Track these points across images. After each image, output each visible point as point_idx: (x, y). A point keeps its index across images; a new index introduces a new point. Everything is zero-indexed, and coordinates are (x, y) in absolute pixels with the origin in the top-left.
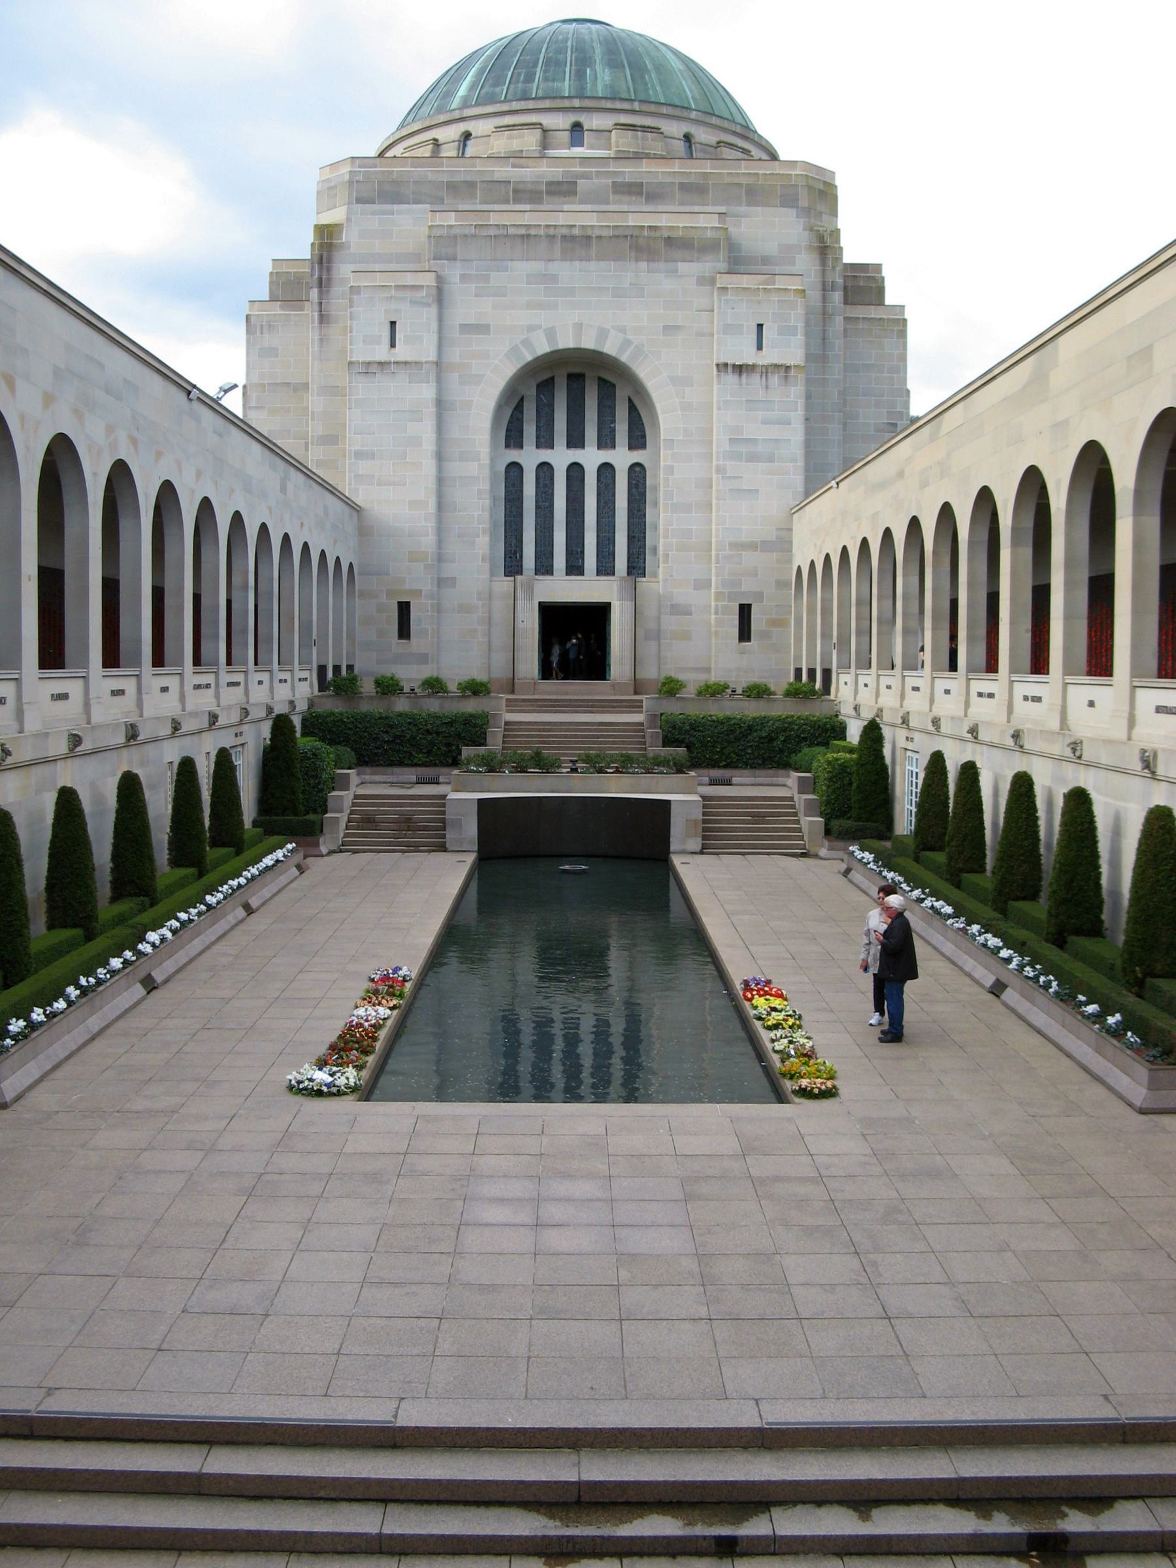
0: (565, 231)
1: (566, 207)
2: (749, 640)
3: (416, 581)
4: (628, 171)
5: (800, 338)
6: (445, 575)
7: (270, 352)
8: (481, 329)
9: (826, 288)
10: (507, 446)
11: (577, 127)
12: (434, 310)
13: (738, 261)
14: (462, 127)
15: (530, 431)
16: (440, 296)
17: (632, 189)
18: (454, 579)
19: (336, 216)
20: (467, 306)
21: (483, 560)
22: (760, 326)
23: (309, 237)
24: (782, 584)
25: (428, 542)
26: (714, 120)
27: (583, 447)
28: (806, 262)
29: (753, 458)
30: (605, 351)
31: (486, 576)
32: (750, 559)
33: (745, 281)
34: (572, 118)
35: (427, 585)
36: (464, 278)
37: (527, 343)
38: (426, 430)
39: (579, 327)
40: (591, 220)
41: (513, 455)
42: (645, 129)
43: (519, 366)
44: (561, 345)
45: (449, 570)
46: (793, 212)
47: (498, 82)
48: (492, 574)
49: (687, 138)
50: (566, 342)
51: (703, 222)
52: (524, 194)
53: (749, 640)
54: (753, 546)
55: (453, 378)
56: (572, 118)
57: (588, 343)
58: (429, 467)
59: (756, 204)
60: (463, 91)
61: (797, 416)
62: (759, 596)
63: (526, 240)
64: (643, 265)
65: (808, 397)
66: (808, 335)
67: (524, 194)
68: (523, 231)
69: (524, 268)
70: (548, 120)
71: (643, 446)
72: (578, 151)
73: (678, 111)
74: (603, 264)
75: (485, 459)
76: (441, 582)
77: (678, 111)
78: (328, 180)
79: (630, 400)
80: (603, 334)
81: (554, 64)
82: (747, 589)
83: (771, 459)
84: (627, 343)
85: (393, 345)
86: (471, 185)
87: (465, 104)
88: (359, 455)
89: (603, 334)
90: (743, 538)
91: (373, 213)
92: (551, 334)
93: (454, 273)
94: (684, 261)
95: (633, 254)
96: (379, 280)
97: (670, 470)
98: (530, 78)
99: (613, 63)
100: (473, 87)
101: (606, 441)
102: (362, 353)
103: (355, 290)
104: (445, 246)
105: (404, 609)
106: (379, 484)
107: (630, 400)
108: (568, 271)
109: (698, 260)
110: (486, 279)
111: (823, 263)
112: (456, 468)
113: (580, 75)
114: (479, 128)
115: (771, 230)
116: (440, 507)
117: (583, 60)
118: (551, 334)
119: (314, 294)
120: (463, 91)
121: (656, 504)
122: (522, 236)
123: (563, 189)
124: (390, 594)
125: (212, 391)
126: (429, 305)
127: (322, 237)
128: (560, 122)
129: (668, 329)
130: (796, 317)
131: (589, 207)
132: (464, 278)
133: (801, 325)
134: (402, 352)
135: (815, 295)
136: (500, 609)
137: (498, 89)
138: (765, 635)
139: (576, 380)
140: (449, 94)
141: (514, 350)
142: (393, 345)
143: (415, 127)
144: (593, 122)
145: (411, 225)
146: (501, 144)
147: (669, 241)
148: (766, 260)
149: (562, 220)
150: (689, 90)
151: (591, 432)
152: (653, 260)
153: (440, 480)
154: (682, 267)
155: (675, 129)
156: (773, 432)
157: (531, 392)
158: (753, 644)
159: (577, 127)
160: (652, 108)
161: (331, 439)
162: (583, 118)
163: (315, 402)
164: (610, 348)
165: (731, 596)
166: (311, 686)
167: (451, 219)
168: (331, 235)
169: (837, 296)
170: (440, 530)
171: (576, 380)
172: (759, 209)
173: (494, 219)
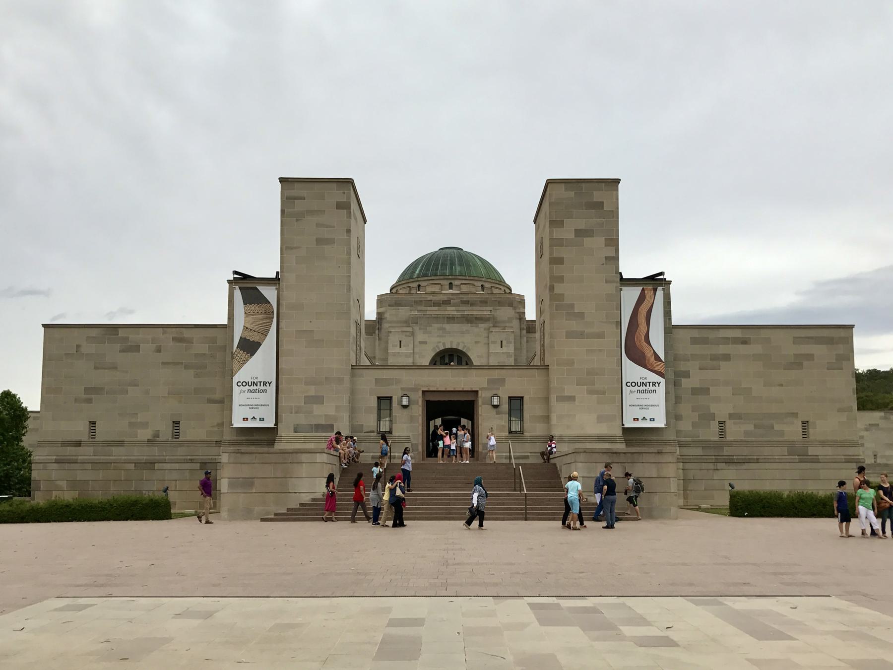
1: (448, 308)
4: (465, 298)
8: (425, 343)
9: (521, 329)
11: (451, 284)
13: (495, 322)
16: (413, 334)
20: (420, 337)
28: (516, 323)
33: (497, 329)
36: (420, 329)
39: (451, 342)
47: (428, 270)
50: (448, 346)
52: (435, 304)
55: (417, 356)
60: (417, 272)
63: (437, 318)
67: (435, 304)
69: (436, 326)
70: (442, 282)
73: (479, 278)
77: (479, 278)
80: (459, 344)
81: (444, 265)
87: (418, 277)
89: (459, 344)
92: (444, 344)
93: (417, 328)
99: (461, 265)
100: (420, 271)
104: (415, 321)
108: (448, 327)
113: (451, 268)
114: (423, 284)
118: (444, 344)
120: (417, 272)
123: (447, 303)
128: (447, 283)
129: (476, 342)
130: (512, 338)
131: (454, 308)
132: (420, 329)
135: (518, 331)
140: (414, 272)
144: (456, 283)
145: (404, 312)
146: (430, 289)
147: (476, 318)
148: (504, 322)
149: (447, 312)
150: (483, 271)
154: (480, 325)
159: (451, 284)
164: (460, 348)
167: (416, 313)
169: (524, 332)
173: (428, 313)
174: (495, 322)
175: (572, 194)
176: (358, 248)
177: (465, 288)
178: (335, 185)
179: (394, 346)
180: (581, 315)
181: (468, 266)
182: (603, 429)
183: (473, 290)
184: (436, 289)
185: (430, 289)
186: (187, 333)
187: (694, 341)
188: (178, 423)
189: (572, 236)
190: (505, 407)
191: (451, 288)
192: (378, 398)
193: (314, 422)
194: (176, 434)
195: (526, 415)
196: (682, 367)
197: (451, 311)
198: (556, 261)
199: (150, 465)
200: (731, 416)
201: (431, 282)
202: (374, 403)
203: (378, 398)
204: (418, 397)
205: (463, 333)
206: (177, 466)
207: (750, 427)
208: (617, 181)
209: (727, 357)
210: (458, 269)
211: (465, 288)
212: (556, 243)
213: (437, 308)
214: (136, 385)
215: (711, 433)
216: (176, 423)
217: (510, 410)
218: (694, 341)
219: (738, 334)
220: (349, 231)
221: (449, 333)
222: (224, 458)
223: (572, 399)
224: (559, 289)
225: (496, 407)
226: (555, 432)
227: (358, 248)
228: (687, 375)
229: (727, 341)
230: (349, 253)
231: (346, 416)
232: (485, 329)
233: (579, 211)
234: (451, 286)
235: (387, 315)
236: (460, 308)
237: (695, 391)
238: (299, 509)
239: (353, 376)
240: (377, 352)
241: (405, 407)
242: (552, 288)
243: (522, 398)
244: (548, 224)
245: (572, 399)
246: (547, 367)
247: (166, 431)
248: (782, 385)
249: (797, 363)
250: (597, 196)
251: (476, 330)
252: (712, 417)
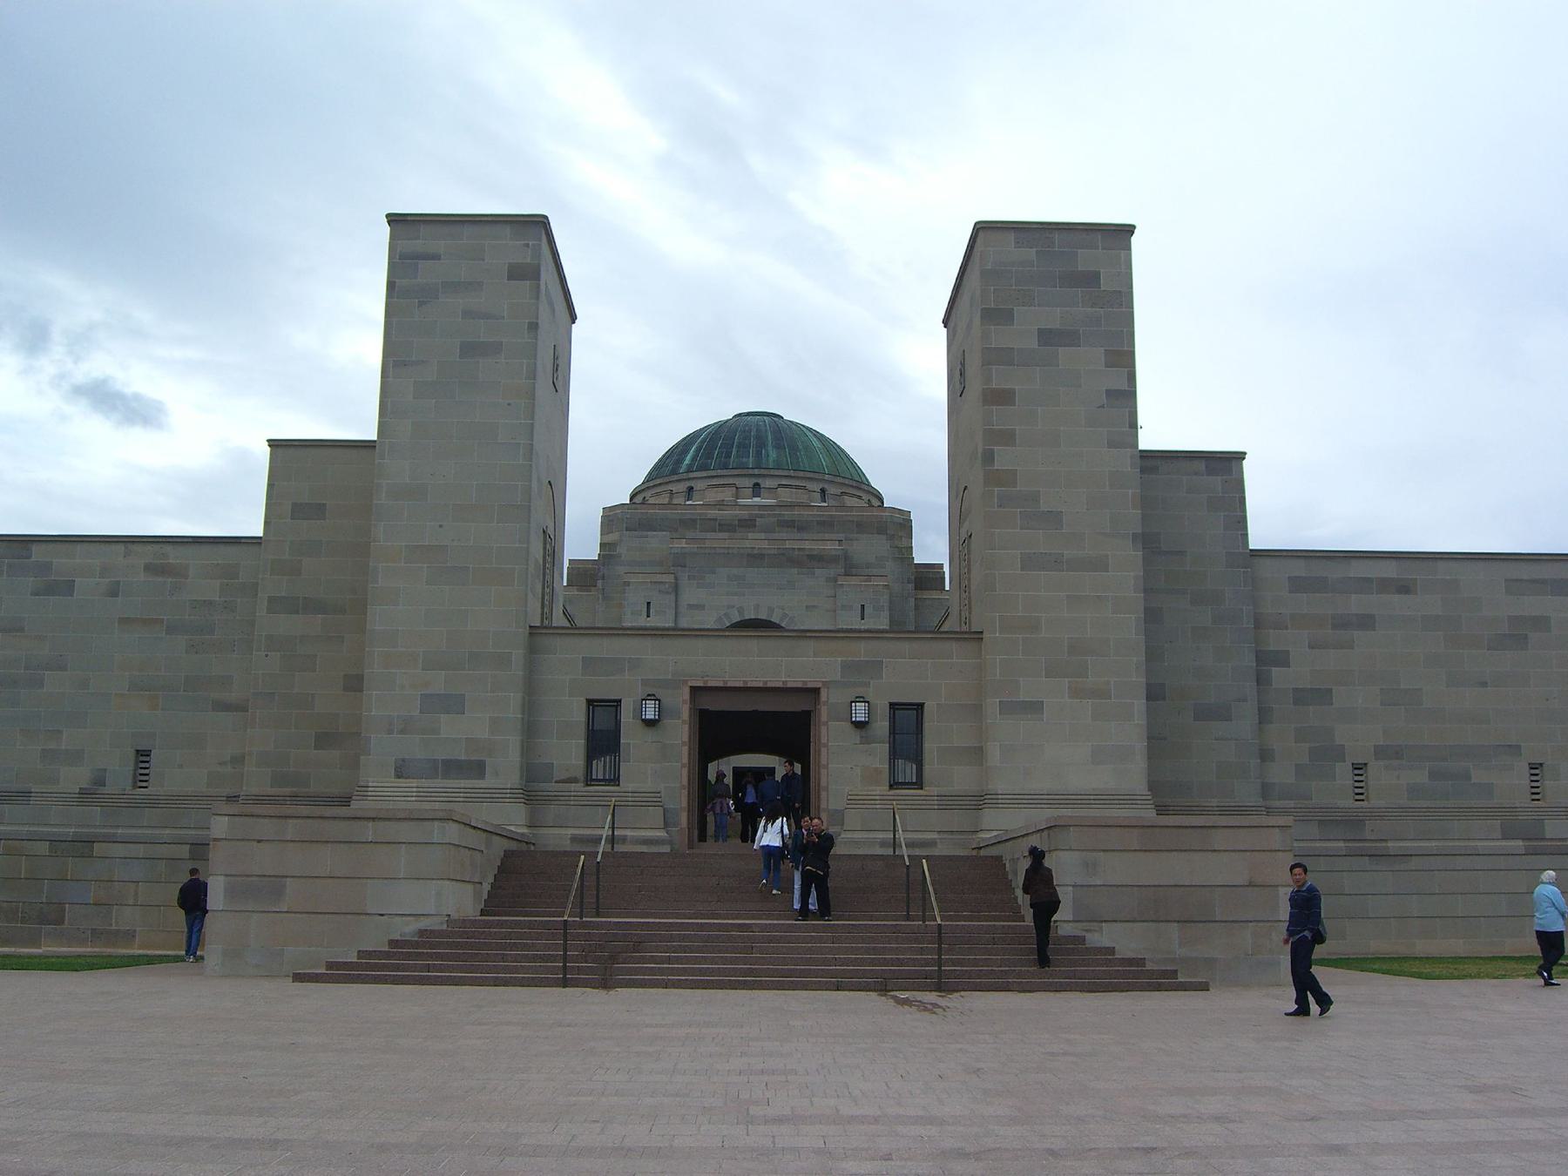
1: (750, 535)
5: (886, 613)
8: (700, 607)
11: (757, 485)
12: (673, 597)
14: (688, 484)
16: (676, 588)
17: (790, 524)
19: (611, 538)
20: (690, 594)
26: (839, 480)
33: (854, 581)
34: (755, 480)
39: (757, 607)
40: (765, 545)
42: (797, 487)
47: (709, 455)
49: (823, 491)
51: (829, 546)
56: (755, 480)
70: (738, 482)
72: (757, 499)
80: (771, 610)
81: (744, 447)
84: (785, 615)
86: (694, 521)
87: (689, 470)
89: (771, 610)
92: (741, 610)
96: (640, 578)
98: (728, 456)
99: (778, 447)
100: (694, 459)
103: (628, 584)
104: (679, 561)
113: (758, 454)
114: (698, 485)
115: (868, 548)
117: (761, 444)
118: (741, 610)
123: (748, 524)
131: (763, 536)
133: (886, 605)
140: (679, 461)
143: (658, 481)
144: (768, 483)
145: (656, 542)
146: (713, 496)
147: (811, 557)
148: (868, 566)
149: (748, 544)
155: (817, 487)
159: (757, 485)
160: (801, 474)
162: (760, 481)
174: (850, 567)
175: (1031, 253)
176: (556, 368)
177: (786, 495)
178: (508, 230)
180: (1054, 518)
181: (794, 449)
182: (1102, 779)
183: (802, 497)
184: (727, 495)
185: (713, 496)
186: (174, 556)
187: (1298, 585)
188: (147, 753)
189: (1033, 343)
190: (882, 726)
191: (756, 494)
192: (590, 702)
193: (441, 755)
194: (141, 776)
195: (930, 746)
196: (1274, 641)
197: (754, 541)
198: (998, 397)
199: (84, 845)
200: (1380, 752)
201: (715, 481)
202: (579, 714)
203: (590, 702)
204: (681, 702)
206: (140, 850)
207: (1420, 777)
208: (1129, 230)
209: (1366, 622)
210: (773, 454)
211: (786, 495)
212: (997, 357)
213: (726, 535)
214: (63, 668)
215: (1336, 790)
216: (143, 755)
217: (893, 731)
218: (1298, 585)
219: (1390, 570)
220: (534, 327)
222: (220, 826)
223: (1035, 707)
224: (1005, 458)
225: (859, 725)
226: (1000, 785)
227: (556, 368)
228: (1282, 660)
229: (1364, 585)
230: (533, 375)
231: (512, 743)
233: (1045, 302)
234: (757, 490)
236: (776, 536)
237: (1301, 697)
238: (387, 955)
239: (532, 650)
241: (650, 723)
242: (989, 457)
243: (921, 705)
244: (977, 320)
245: (1035, 707)
246: (978, 636)
247: (120, 768)
248: (1484, 684)
249: (1517, 635)
250: (1086, 260)
252: (1339, 754)
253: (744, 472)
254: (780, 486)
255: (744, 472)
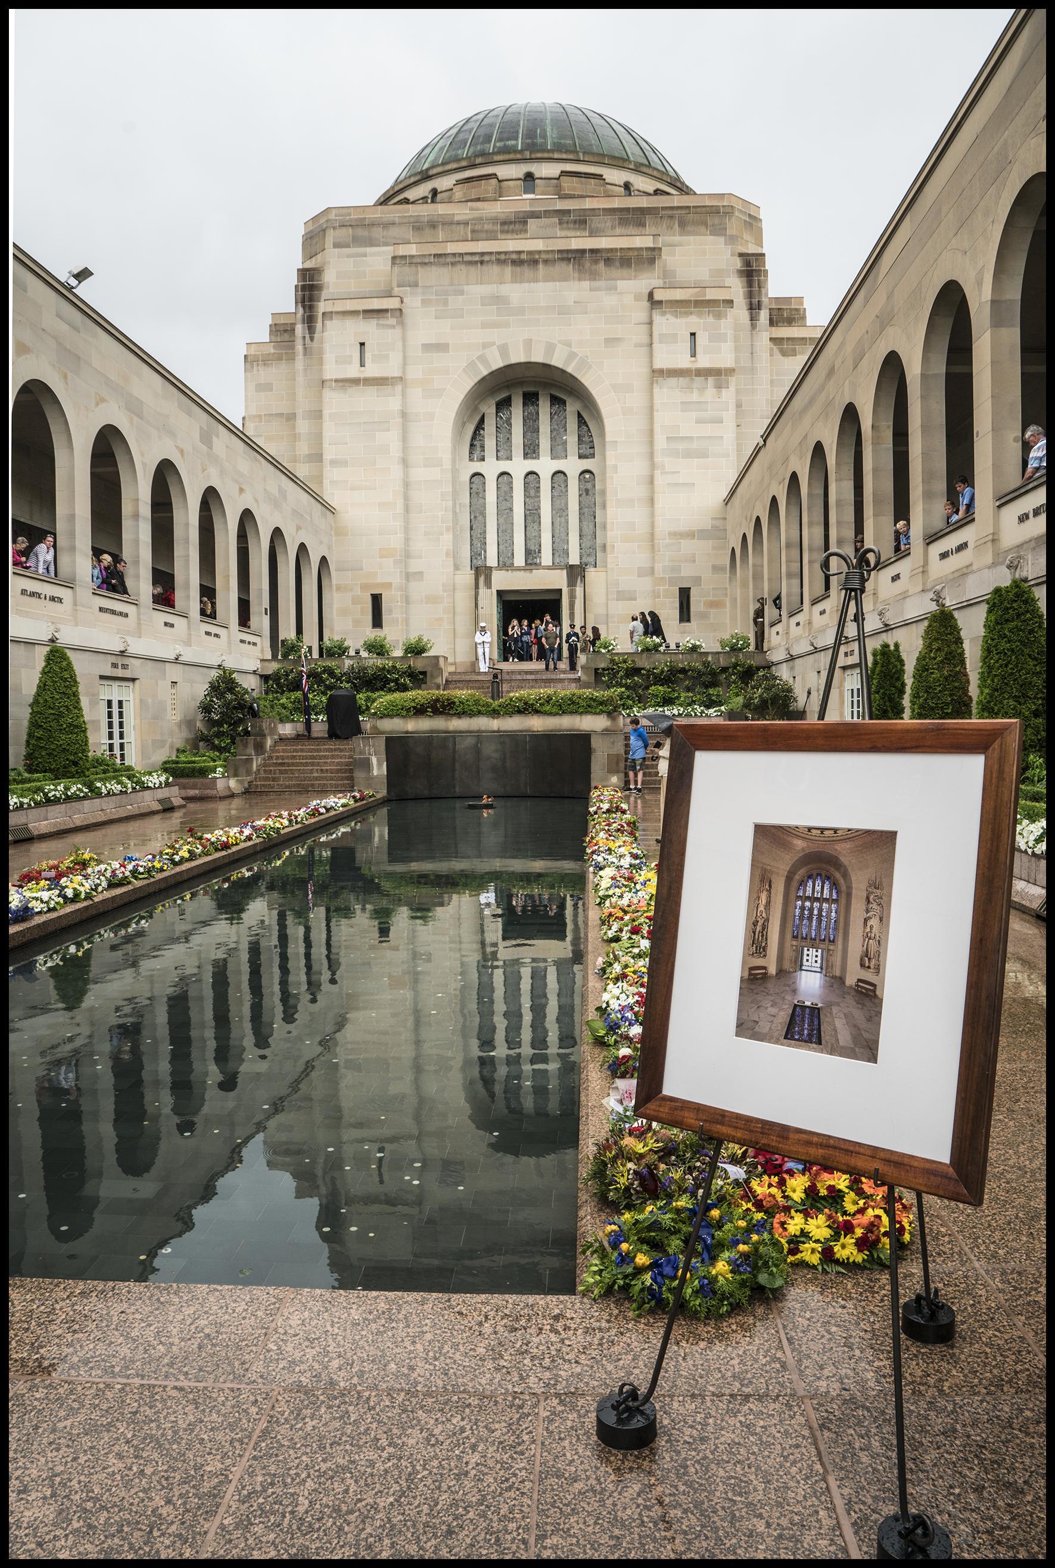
0: (514, 256)
2: (689, 620)
3: (385, 575)
6: (412, 569)
7: (266, 387)
8: (441, 347)
10: (471, 460)
15: (490, 443)
18: (421, 573)
21: (447, 555)
22: (693, 334)
23: (293, 280)
24: (716, 569)
25: (396, 541)
27: (537, 457)
29: (688, 454)
30: (553, 363)
31: (452, 569)
32: (688, 546)
35: (396, 580)
37: (482, 358)
38: (392, 438)
39: (528, 344)
41: (477, 467)
43: (476, 380)
44: (514, 360)
45: (415, 566)
46: (722, 239)
48: (457, 567)
53: (689, 620)
54: (691, 535)
57: (538, 357)
58: (396, 471)
59: (689, 234)
61: (729, 416)
62: (698, 580)
64: (586, 284)
65: (739, 406)
66: (736, 339)
68: (477, 258)
71: (593, 456)
74: (550, 284)
75: (447, 464)
76: (408, 576)
78: (311, 231)
79: (579, 413)
80: (550, 348)
82: (687, 573)
83: (704, 454)
84: (572, 356)
85: (362, 365)
88: (334, 463)
89: (550, 348)
90: (683, 527)
91: (348, 256)
92: (503, 350)
94: (623, 279)
95: (576, 275)
97: (616, 467)
98: (488, 139)
101: (558, 451)
102: (332, 370)
105: (376, 600)
106: (351, 489)
107: (579, 415)
109: (635, 278)
110: (445, 303)
111: (750, 284)
112: (418, 473)
116: (407, 509)
118: (503, 350)
119: (299, 329)
121: (604, 507)
122: (476, 262)
124: (364, 587)
125: (63, 275)
126: (393, 327)
127: (304, 280)
129: (610, 342)
133: (730, 333)
134: (372, 370)
136: (463, 600)
137: (460, 152)
138: (704, 616)
139: (531, 399)
141: (471, 365)
142: (362, 365)
151: (545, 443)
152: (595, 280)
153: (406, 485)
154: (620, 283)
156: (708, 430)
157: (489, 409)
158: (694, 624)
161: (317, 457)
163: (303, 426)
164: (557, 361)
165: (672, 582)
166: (262, 651)
168: (312, 279)
170: (406, 530)
171: (531, 399)
172: (692, 238)
179: (342, 360)
205: (563, 311)
221: (521, 311)
232: (637, 298)
235: (330, 279)
240: (300, 392)
251: (608, 300)
253: (511, 156)
254: (564, 173)
255: (511, 156)
